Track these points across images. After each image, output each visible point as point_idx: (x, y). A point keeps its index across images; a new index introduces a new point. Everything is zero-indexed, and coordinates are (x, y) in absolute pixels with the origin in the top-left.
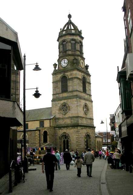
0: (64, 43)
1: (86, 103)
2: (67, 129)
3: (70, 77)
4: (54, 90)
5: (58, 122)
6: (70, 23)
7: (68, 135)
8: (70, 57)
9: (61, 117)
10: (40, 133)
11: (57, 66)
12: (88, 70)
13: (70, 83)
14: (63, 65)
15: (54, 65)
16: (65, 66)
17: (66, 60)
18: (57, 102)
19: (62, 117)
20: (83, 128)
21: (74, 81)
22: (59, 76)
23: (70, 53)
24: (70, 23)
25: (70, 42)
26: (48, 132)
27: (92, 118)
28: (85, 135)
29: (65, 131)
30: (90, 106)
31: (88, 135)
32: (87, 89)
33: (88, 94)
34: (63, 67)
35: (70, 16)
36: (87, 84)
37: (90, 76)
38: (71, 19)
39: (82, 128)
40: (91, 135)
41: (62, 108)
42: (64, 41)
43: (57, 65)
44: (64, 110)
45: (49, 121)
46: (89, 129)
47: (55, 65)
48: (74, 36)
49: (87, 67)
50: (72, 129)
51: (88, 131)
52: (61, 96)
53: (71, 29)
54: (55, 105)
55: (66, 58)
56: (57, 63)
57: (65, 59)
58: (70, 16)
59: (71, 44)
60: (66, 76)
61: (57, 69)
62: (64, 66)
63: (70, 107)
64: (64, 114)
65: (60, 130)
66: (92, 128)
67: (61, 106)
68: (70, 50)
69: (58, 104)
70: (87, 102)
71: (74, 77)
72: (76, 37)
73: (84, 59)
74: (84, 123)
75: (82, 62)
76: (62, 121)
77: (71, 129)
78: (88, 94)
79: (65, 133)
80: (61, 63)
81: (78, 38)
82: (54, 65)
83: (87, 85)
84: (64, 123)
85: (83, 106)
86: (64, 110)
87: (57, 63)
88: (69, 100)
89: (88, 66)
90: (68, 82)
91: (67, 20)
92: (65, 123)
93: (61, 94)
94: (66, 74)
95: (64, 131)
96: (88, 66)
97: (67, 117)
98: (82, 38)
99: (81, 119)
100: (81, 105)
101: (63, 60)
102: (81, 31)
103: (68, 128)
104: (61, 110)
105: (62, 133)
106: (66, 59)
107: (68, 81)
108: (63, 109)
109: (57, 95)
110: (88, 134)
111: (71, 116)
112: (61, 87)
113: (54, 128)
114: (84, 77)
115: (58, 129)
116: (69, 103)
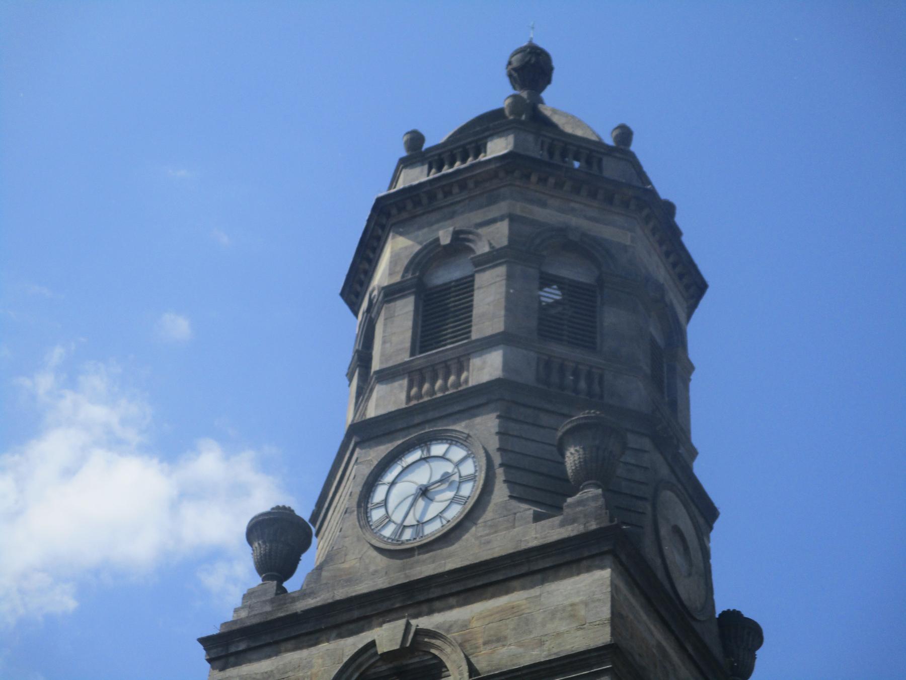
17: (458, 453)
57: (438, 449)
61: (292, 585)
75: (677, 531)
80: (379, 494)
106: (452, 440)
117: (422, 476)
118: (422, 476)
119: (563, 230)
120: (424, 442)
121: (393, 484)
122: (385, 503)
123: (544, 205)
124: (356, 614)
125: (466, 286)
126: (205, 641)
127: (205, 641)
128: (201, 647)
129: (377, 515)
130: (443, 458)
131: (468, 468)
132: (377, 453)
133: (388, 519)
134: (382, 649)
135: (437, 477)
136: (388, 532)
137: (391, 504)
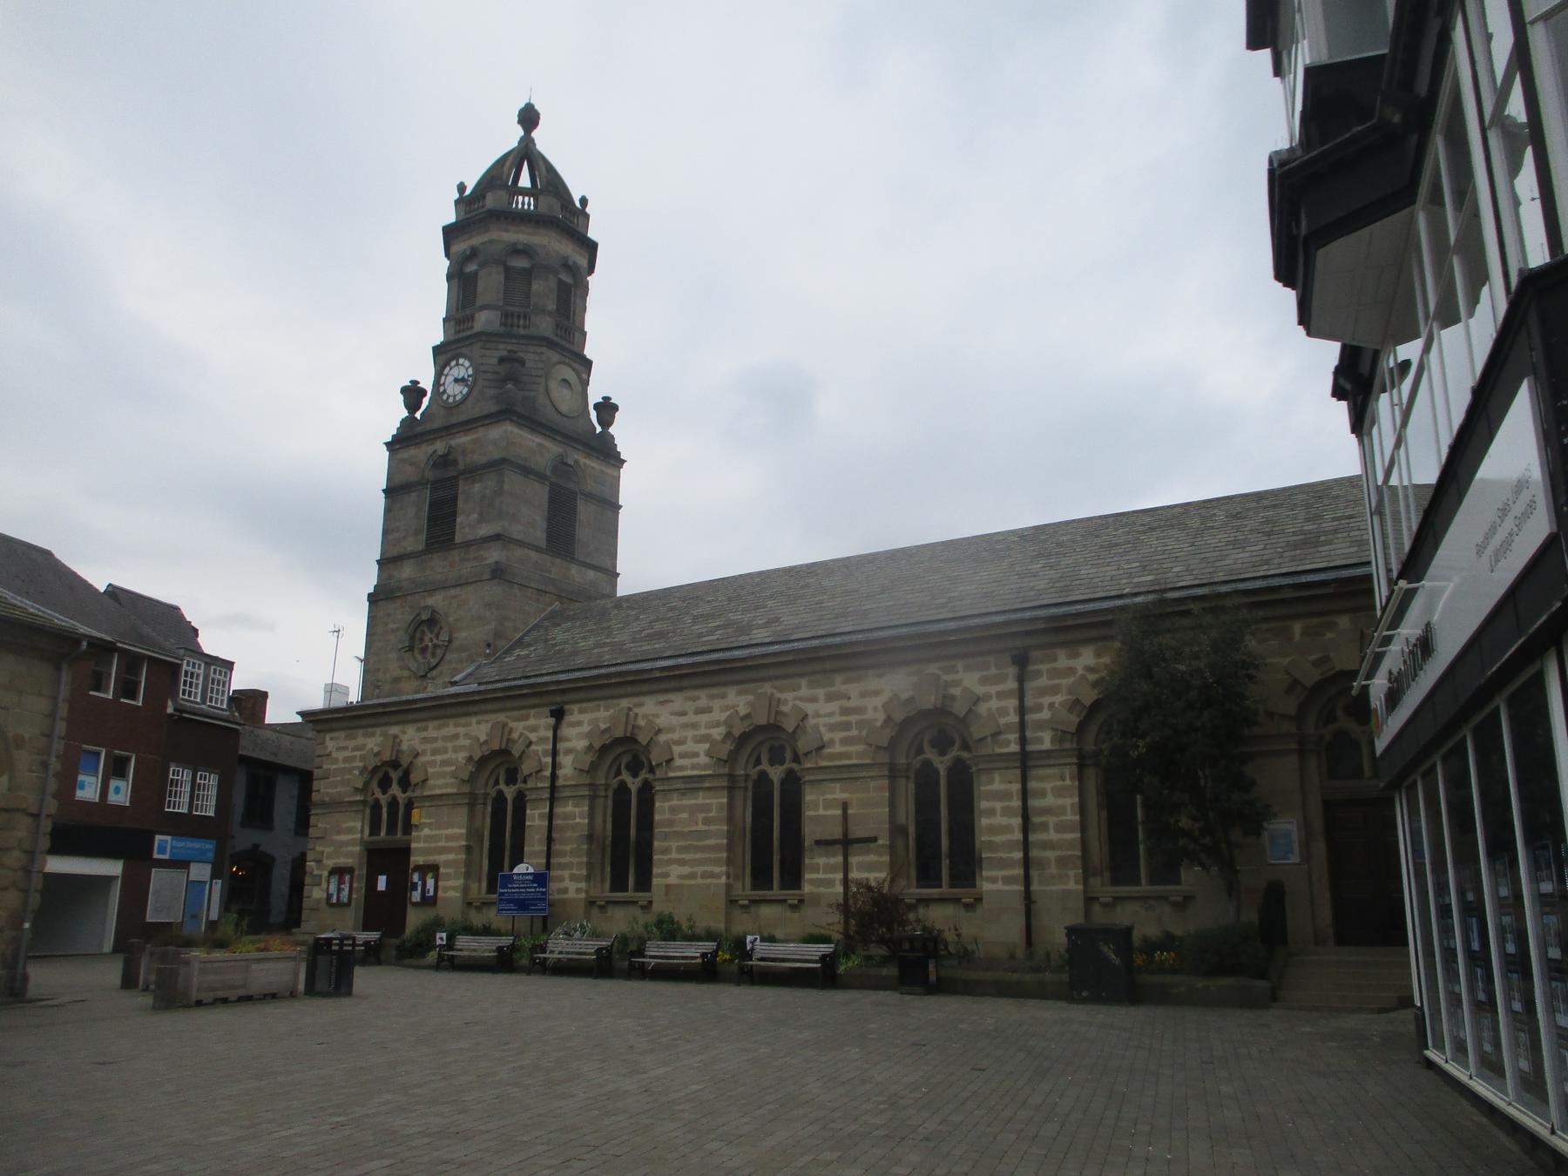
0: (471, 267)
6: (526, 153)
11: (426, 402)
12: (612, 430)
13: (471, 493)
14: (449, 391)
15: (404, 390)
16: (458, 398)
17: (467, 364)
22: (420, 453)
24: (526, 153)
32: (583, 533)
35: (529, 118)
37: (618, 462)
38: (535, 134)
42: (472, 254)
43: (423, 393)
44: (424, 650)
47: (412, 394)
49: (607, 409)
53: (518, 191)
55: (464, 350)
56: (427, 383)
57: (461, 361)
58: (529, 118)
59: (508, 271)
61: (418, 415)
62: (451, 400)
73: (588, 364)
81: (552, 244)
82: (404, 390)
83: (585, 511)
86: (427, 646)
87: (427, 383)
89: (615, 408)
91: (512, 136)
96: (615, 408)
98: (591, 248)
101: (454, 363)
102: (584, 201)
104: (411, 648)
106: (466, 357)
108: (422, 640)
119: (515, 244)
120: (457, 357)
121: (446, 376)
122: (444, 384)
123: (507, 231)
124: (432, 437)
125: (475, 275)
126: (387, 444)
127: (387, 444)
128: (384, 446)
129: (442, 389)
131: (470, 371)
133: (445, 391)
134: (440, 453)
137: (447, 384)
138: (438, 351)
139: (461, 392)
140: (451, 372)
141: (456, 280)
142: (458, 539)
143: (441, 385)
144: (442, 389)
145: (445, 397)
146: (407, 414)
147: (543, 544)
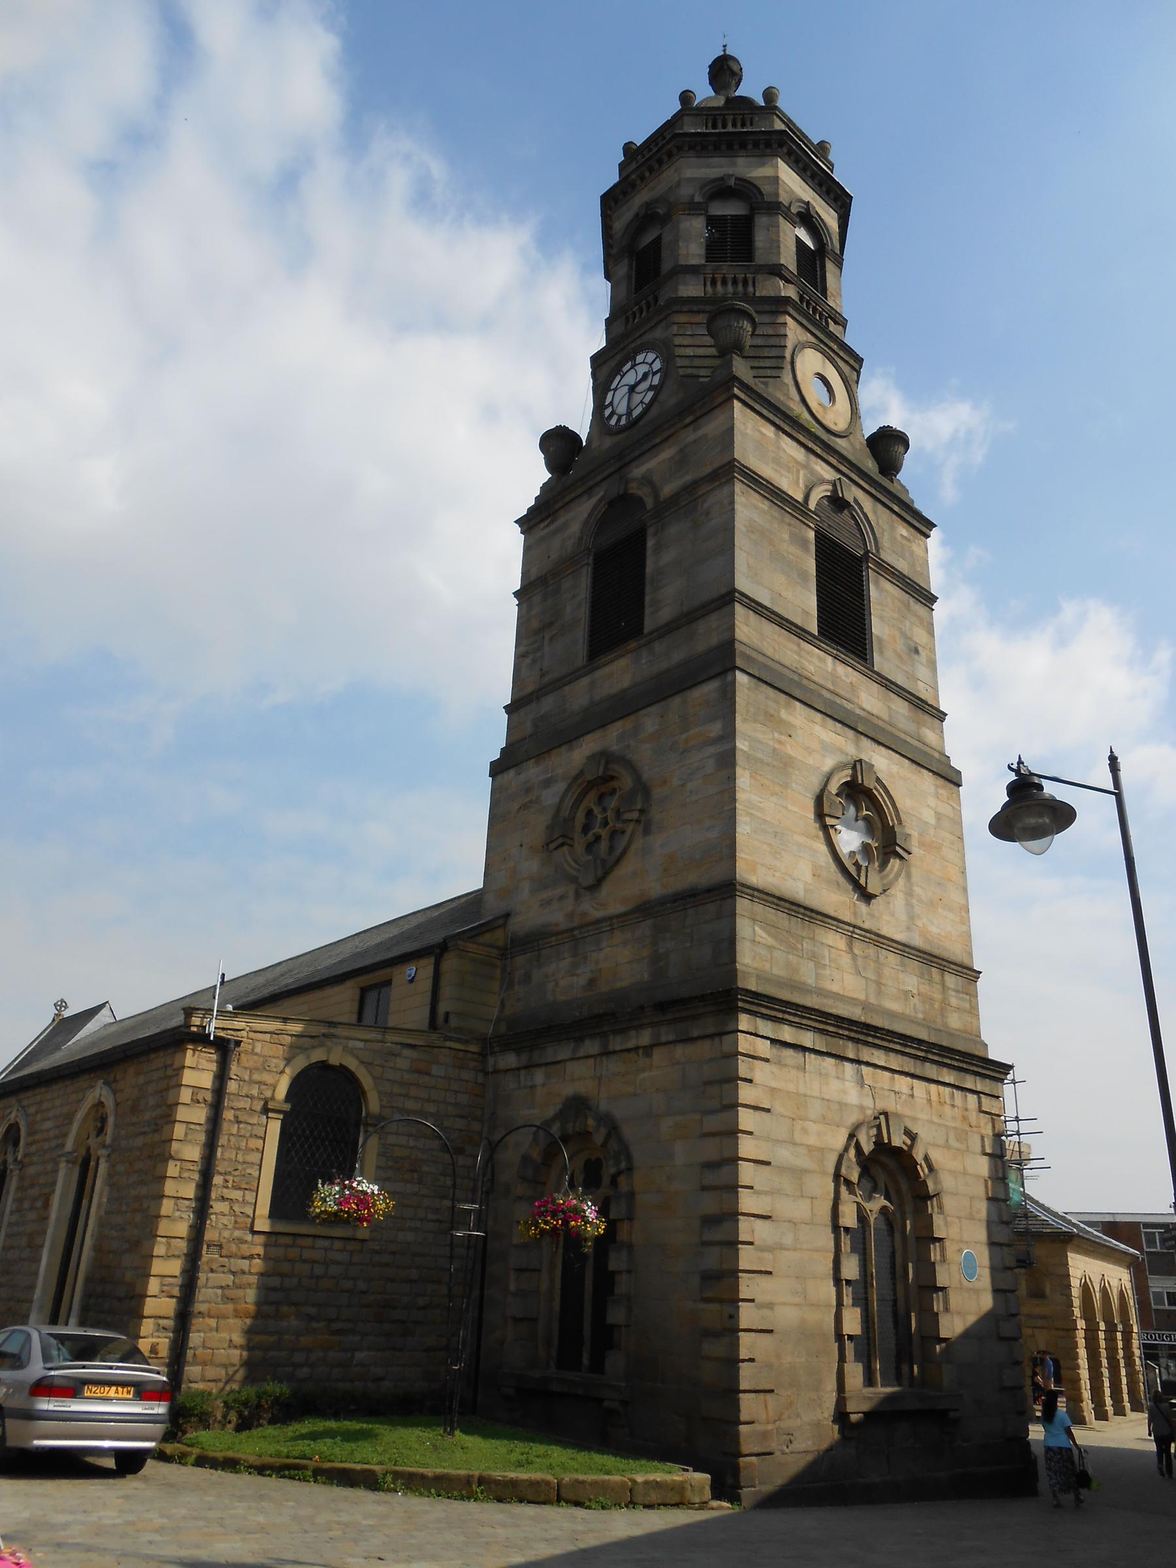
1: (857, 765)
2: (606, 1053)
3: (667, 490)
4: (528, 661)
5: (527, 978)
7: (613, 1128)
8: (682, 318)
9: (556, 916)
10: (222, 1077)
16: (636, 413)
17: (651, 356)
18: (533, 772)
19: (571, 916)
20: (808, 1039)
21: (708, 513)
23: (691, 289)
25: (693, 208)
26: (366, 1081)
27: (954, 951)
28: (839, 1140)
29: (583, 1087)
30: (928, 816)
31: (882, 1147)
33: (888, 685)
34: (622, 430)
36: (888, 586)
39: (787, 1033)
40: (936, 1156)
41: (580, 817)
42: (649, 218)
45: (423, 970)
46: (903, 1083)
48: (741, 161)
50: (658, 1055)
51: (890, 1105)
52: (579, 695)
54: (515, 806)
57: (640, 358)
60: (634, 489)
62: (623, 422)
63: (657, 793)
64: (589, 880)
65: (539, 1077)
66: (949, 1077)
67: (569, 802)
68: (693, 270)
69: (547, 783)
70: (882, 762)
71: (708, 470)
72: (763, 165)
74: (835, 988)
76: (565, 963)
77: (648, 1050)
78: (888, 685)
79: (578, 1105)
84: (582, 981)
85: (815, 784)
88: (650, 721)
90: (650, 543)
92: (592, 982)
93: (585, 681)
94: (638, 471)
95: (568, 1090)
97: (619, 908)
99: (769, 927)
100: (784, 765)
103: (616, 1043)
105: (550, 1112)
107: (650, 531)
109: (548, 704)
110: (898, 1140)
111: (655, 887)
112: (584, 613)
113: (483, 1055)
114: (837, 502)
115: (510, 1060)
116: (643, 754)
117: (630, 378)
118: (630, 378)
121: (615, 390)
122: (611, 404)
129: (607, 412)
130: (643, 363)
132: (605, 370)
135: (640, 377)
136: (613, 422)
137: (615, 403)
138: (597, 361)
139: (642, 402)
140: (624, 381)
141: (626, 262)
142: (649, 624)
143: (607, 407)
144: (607, 412)
145: (613, 422)
146: (550, 476)
147: (813, 627)
